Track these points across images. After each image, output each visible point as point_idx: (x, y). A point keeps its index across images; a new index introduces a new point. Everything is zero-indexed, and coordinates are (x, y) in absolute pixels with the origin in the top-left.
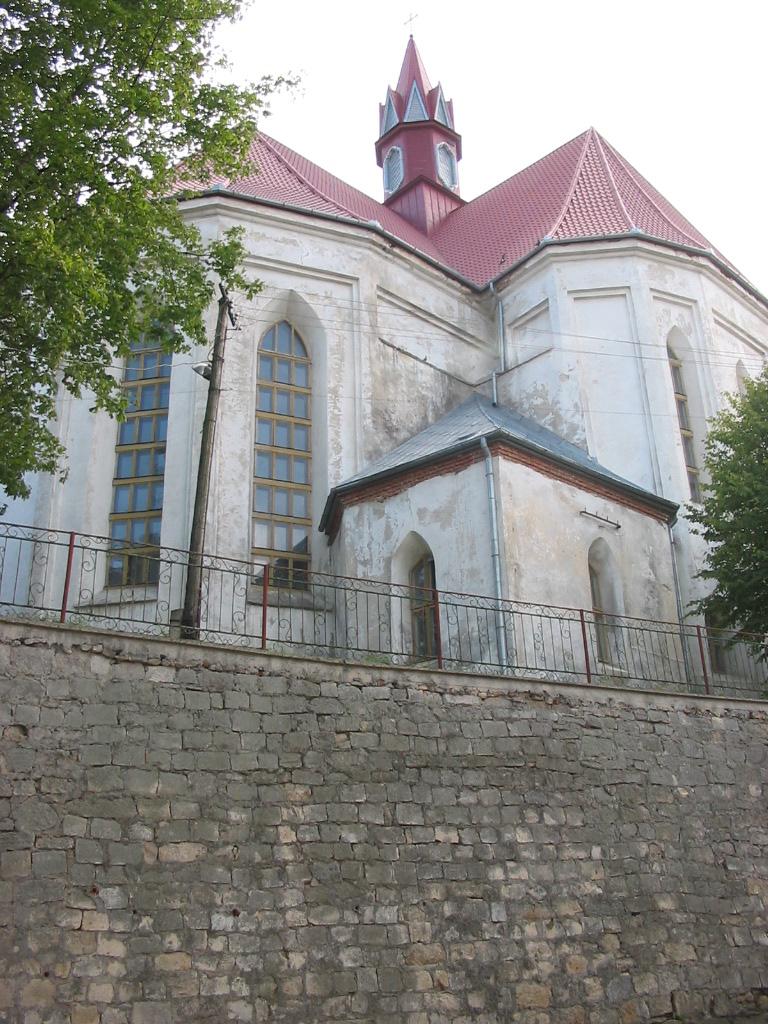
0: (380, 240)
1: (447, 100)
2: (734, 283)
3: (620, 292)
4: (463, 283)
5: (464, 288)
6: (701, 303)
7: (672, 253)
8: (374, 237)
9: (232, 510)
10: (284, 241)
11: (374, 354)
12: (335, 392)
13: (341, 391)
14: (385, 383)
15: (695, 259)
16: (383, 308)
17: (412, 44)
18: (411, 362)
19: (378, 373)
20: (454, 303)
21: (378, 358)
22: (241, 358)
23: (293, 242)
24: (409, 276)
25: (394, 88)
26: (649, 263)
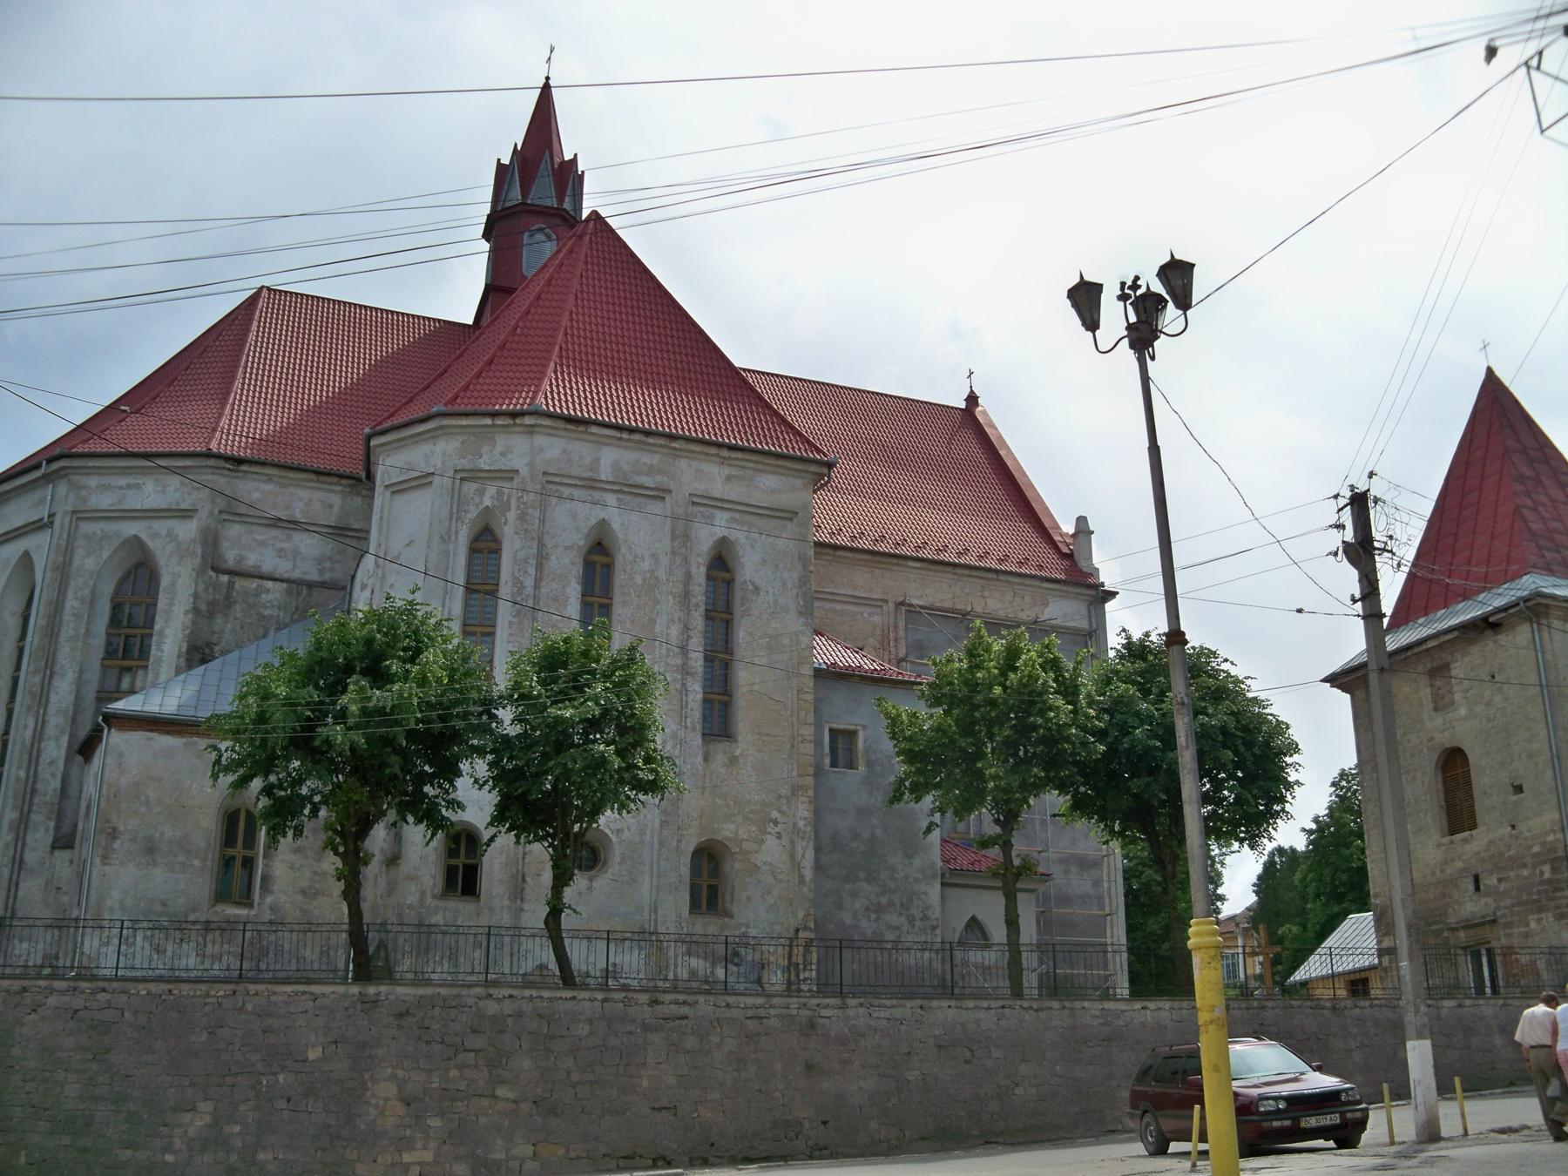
0: (221, 463)
1: (568, 156)
2: (594, 429)
3: (423, 481)
4: (342, 477)
5: (344, 481)
6: (524, 471)
7: (488, 421)
8: (212, 462)
9: (51, 763)
10: (129, 486)
11: (201, 587)
12: (162, 634)
13: (168, 631)
14: (211, 615)
15: (518, 421)
16: (234, 530)
17: (546, 89)
18: (253, 584)
19: (203, 607)
20: (336, 500)
21: (206, 590)
22: (78, 616)
23: (138, 487)
24: (270, 487)
25: (506, 161)
26: (461, 438)
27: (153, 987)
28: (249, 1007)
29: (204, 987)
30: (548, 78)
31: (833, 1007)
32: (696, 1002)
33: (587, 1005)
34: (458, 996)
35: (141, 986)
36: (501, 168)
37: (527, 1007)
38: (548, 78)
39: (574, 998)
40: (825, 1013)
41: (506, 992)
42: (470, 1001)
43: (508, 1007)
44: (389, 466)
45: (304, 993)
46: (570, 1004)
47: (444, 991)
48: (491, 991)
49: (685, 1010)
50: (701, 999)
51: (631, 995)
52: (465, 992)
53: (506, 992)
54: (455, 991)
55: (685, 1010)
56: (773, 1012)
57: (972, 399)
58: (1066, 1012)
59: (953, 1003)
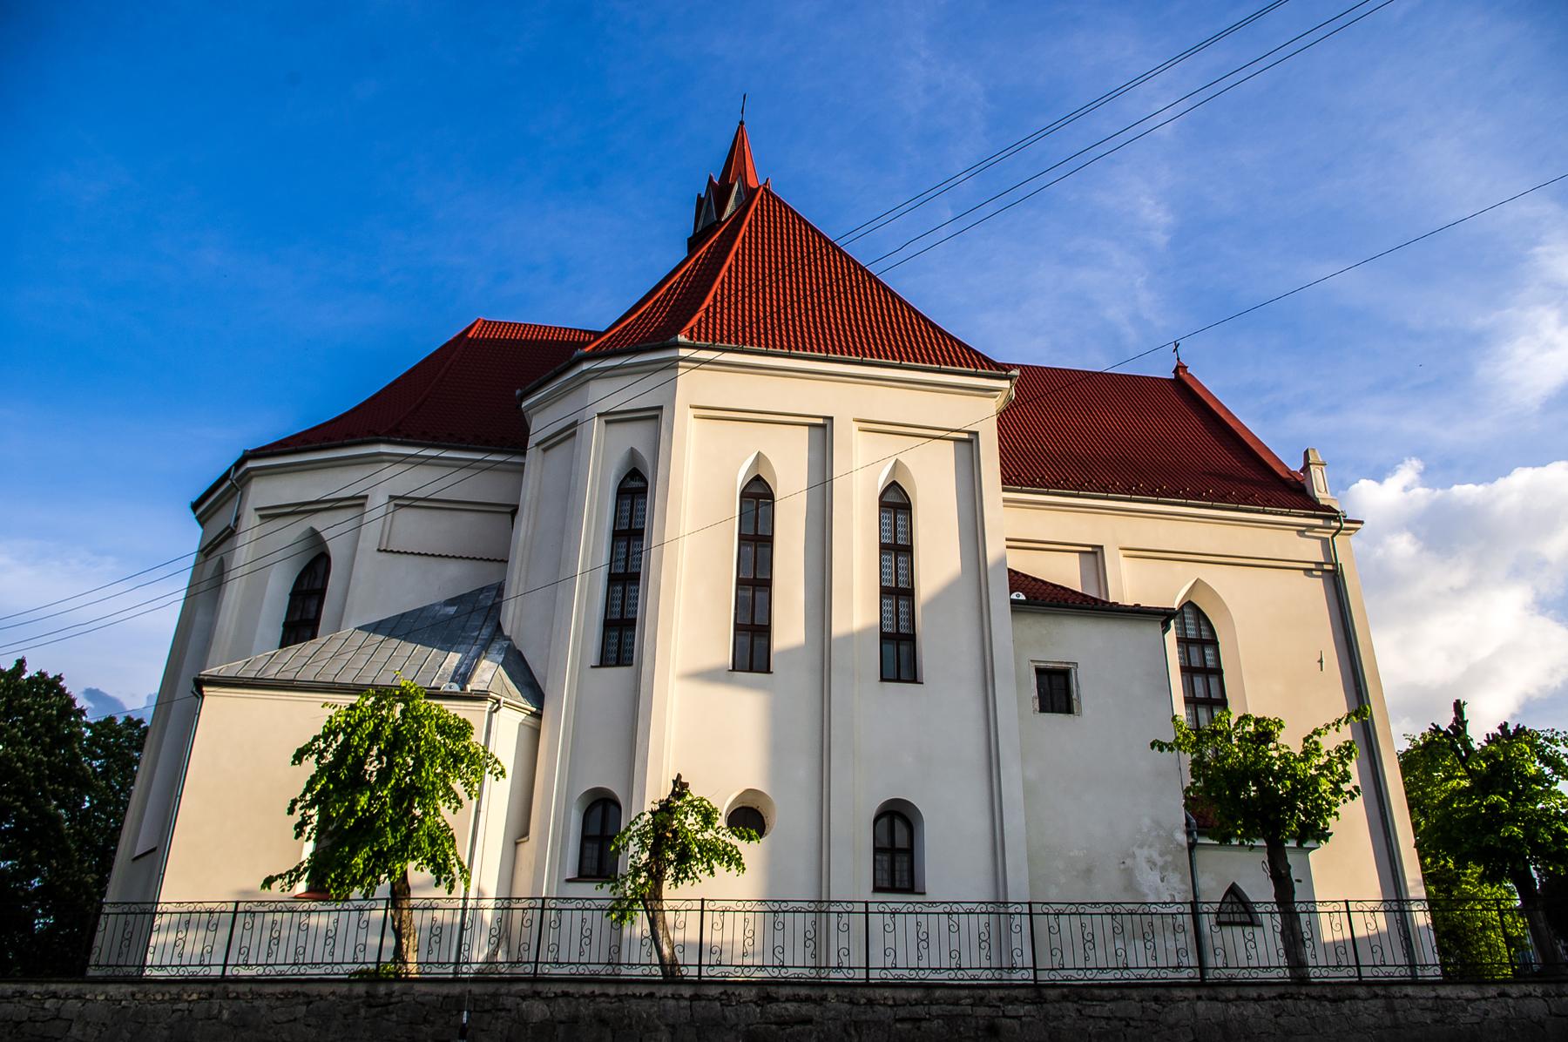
27: (112, 989)
28: (225, 1015)
29: (174, 989)
30: (742, 123)
31: (1024, 1002)
32: (824, 998)
33: (671, 1002)
34: (495, 995)
35: (100, 988)
36: (700, 201)
37: (585, 1010)
38: (742, 123)
39: (651, 995)
40: (1010, 1009)
41: (558, 988)
42: (509, 1002)
43: (563, 1009)
44: (542, 424)
45: (297, 994)
46: (647, 1003)
47: (477, 989)
48: (539, 987)
49: (806, 1009)
50: (831, 993)
51: (730, 990)
52: (504, 989)
53: (558, 988)
54: (491, 988)
55: (806, 1009)
56: (935, 1009)
57: (1180, 368)
58: (1380, 1003)
59: (1204, 992)
